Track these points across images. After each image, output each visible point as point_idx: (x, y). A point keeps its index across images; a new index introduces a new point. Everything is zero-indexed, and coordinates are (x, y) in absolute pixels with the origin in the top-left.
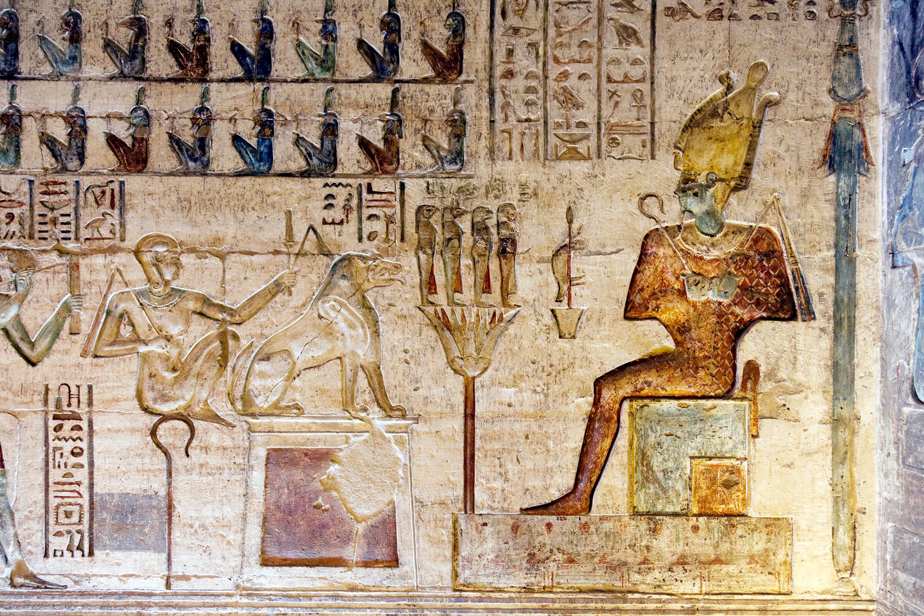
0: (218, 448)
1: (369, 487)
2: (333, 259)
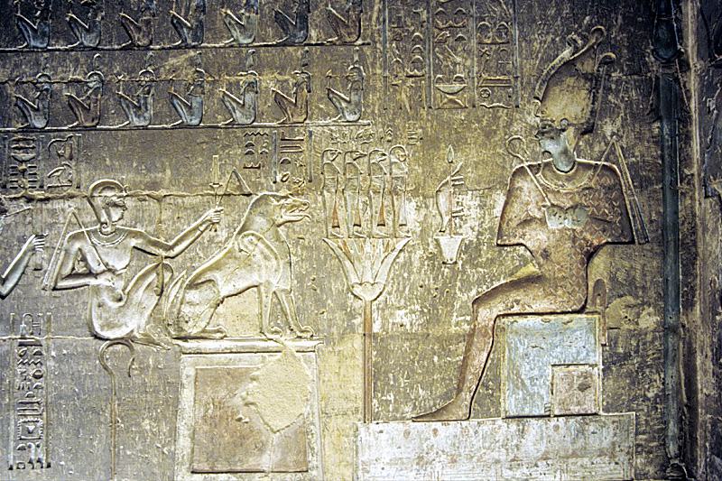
1: (283, 402)
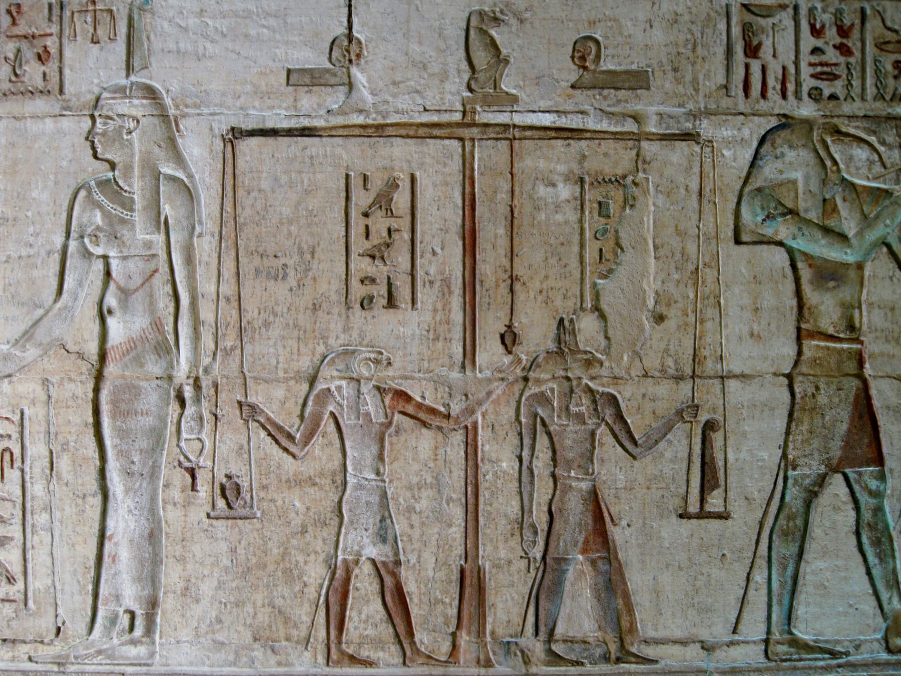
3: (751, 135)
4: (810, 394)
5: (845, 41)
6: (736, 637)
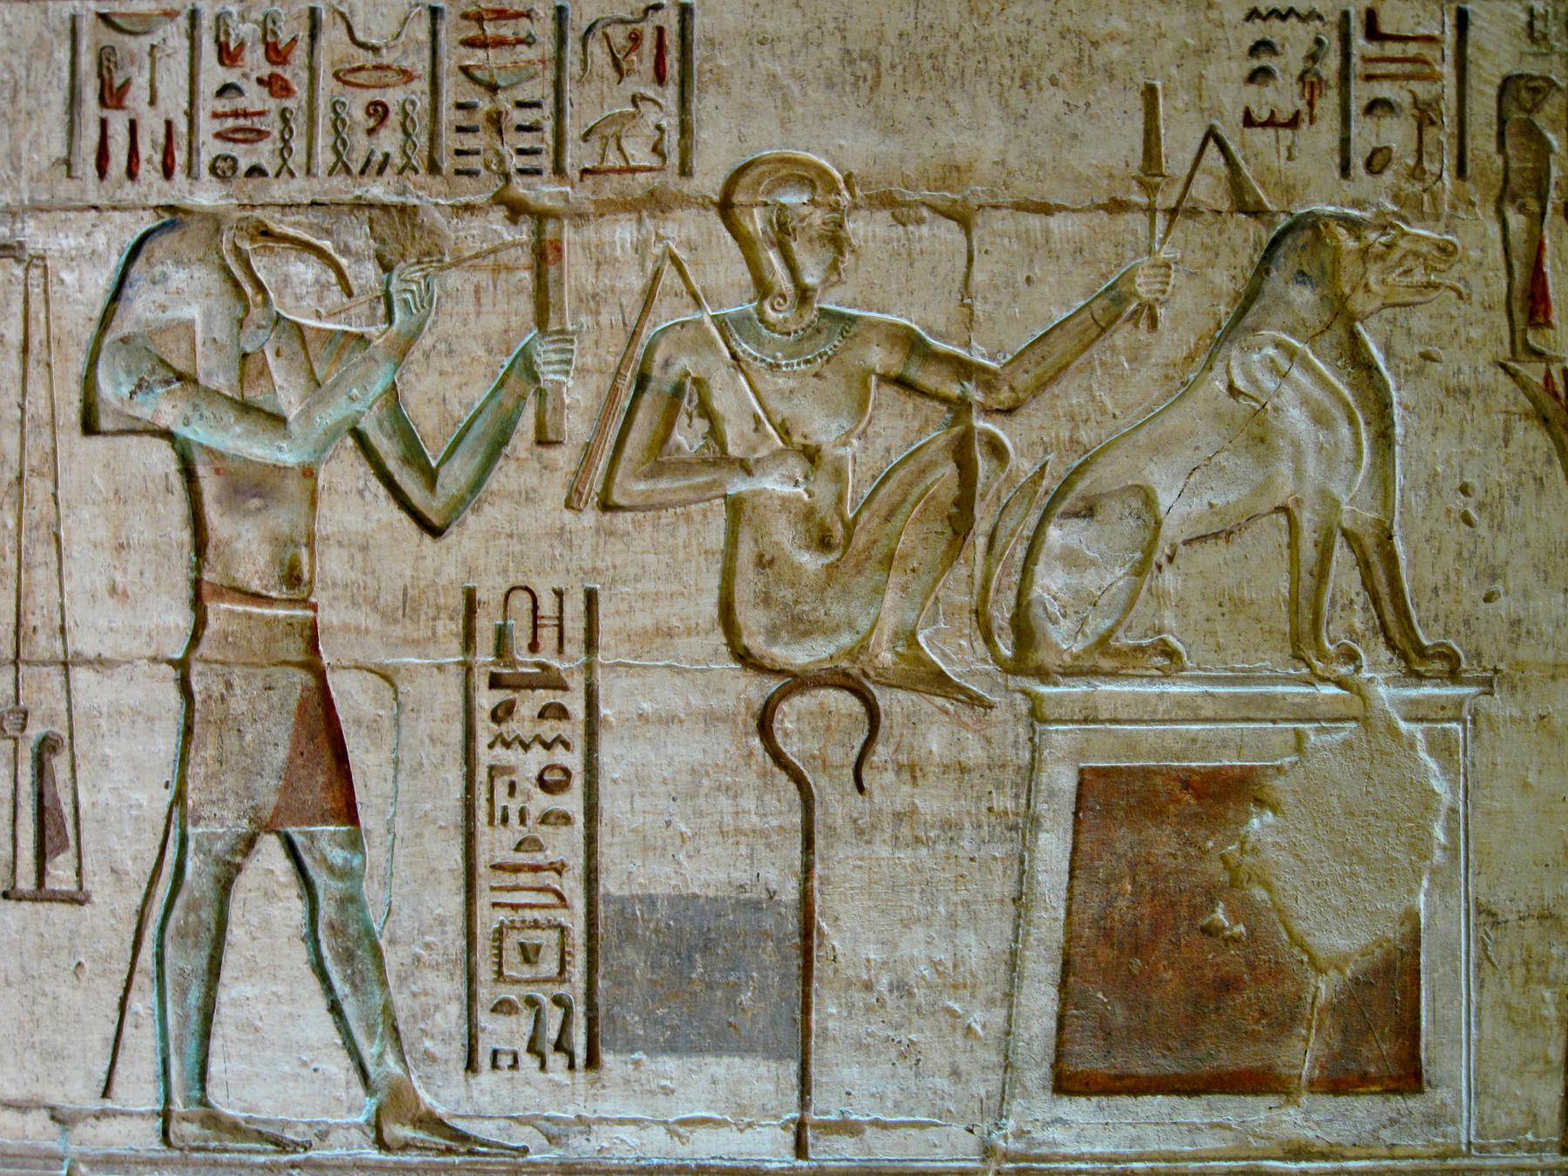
0: (946, 769)
2: (1270, 225)
3: (109, 245)
4: (216, 695)
5: (278, 70)
6: (109, 1104)
